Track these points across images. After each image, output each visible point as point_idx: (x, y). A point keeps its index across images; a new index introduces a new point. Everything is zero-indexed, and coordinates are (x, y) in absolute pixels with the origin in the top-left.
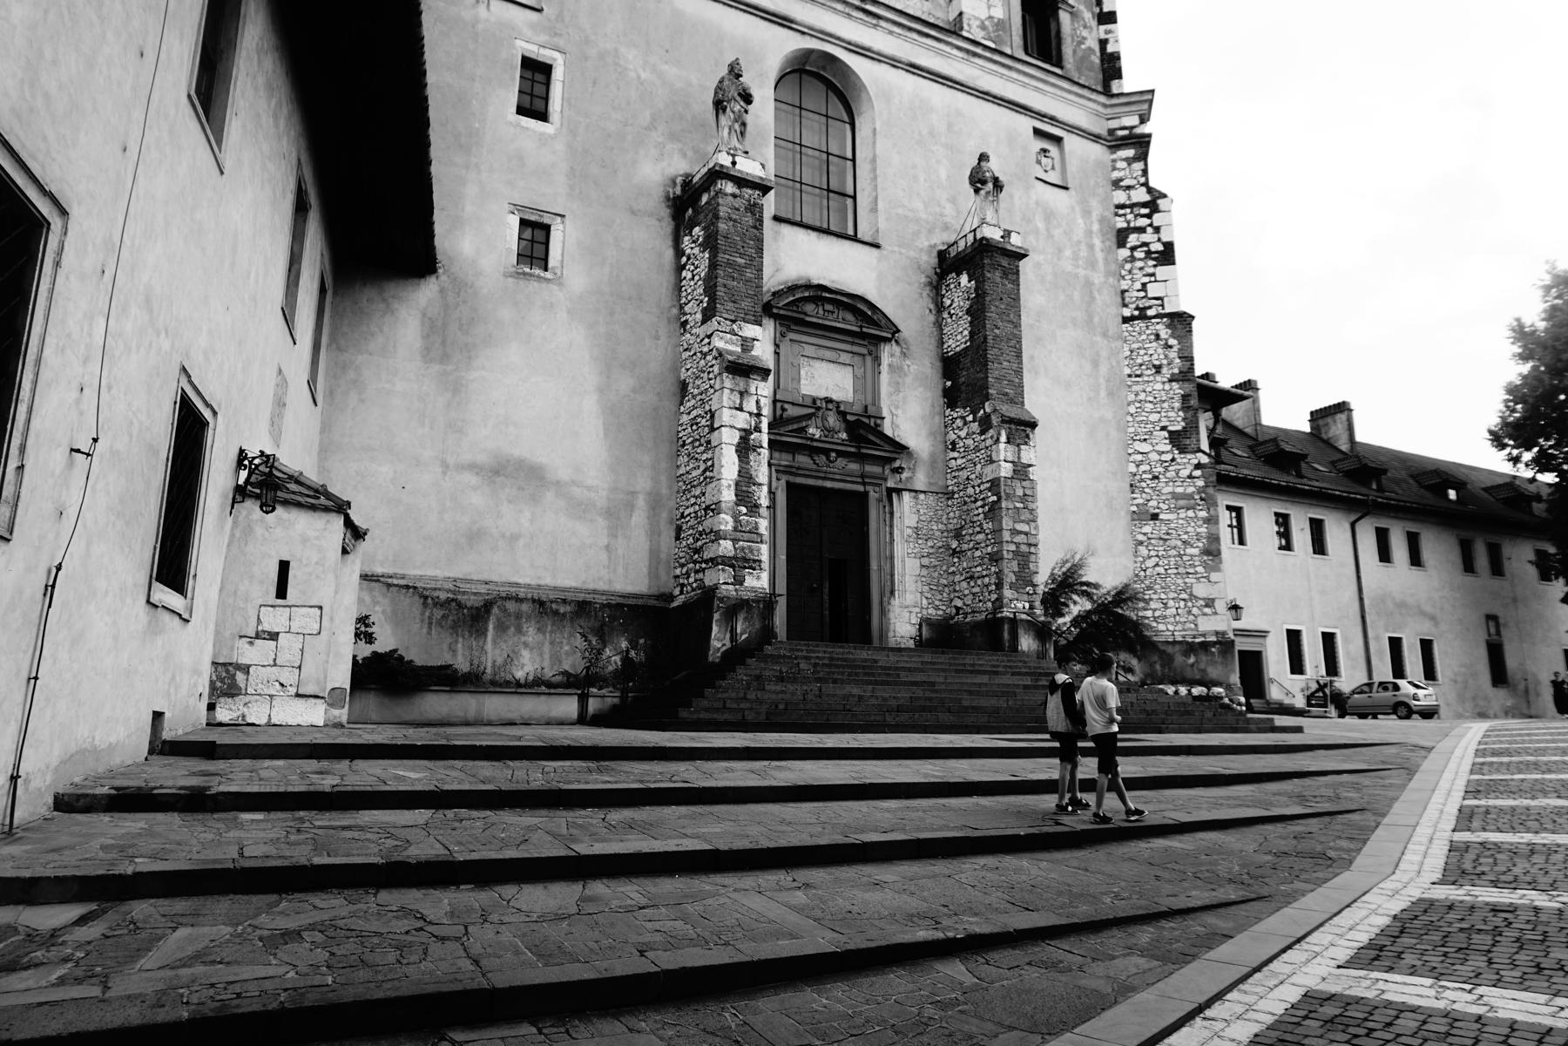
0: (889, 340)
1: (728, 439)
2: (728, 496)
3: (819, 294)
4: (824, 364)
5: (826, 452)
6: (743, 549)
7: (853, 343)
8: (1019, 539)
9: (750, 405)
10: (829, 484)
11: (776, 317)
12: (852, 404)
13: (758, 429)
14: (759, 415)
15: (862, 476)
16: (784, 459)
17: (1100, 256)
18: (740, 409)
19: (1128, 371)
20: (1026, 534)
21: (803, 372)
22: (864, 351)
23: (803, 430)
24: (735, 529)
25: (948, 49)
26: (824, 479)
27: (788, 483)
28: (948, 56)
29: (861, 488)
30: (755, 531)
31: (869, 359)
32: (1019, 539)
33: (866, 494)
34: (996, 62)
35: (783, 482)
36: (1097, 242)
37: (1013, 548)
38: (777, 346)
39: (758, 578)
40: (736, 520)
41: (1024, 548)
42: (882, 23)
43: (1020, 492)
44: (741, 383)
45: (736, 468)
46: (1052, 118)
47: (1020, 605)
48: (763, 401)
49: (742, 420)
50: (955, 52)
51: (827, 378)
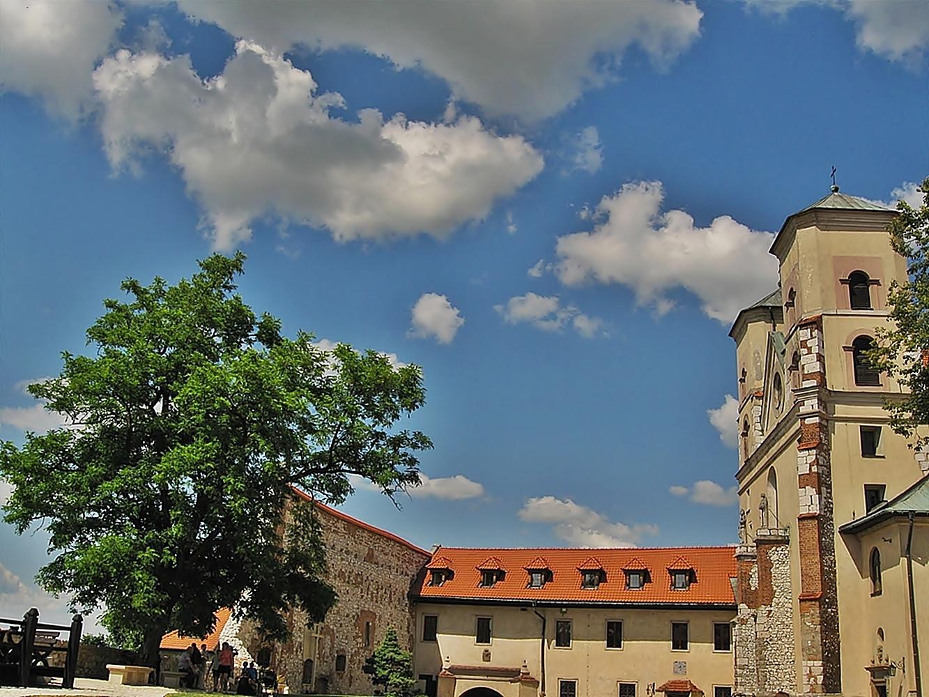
42: (776, 438)
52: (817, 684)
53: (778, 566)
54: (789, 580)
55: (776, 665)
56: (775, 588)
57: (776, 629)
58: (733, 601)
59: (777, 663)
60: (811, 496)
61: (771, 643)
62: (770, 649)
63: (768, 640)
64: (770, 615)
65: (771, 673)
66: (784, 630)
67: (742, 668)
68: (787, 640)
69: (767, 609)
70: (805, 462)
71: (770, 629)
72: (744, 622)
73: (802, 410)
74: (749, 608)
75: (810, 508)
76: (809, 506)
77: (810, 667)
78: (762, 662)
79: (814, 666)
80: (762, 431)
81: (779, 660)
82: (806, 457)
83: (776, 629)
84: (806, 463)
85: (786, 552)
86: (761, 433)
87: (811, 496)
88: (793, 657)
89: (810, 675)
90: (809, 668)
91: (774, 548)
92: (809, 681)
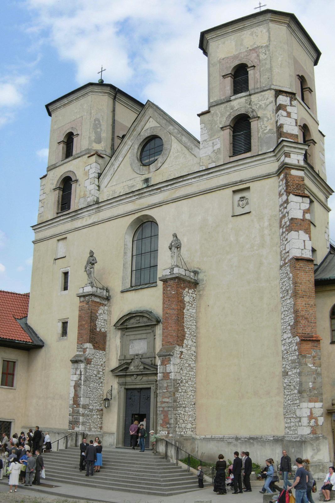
0: (155, 325)
1: (73, 384)
2: (71, 402)
3: (131, 316)
4: (137, 341)
5: (133, 375)
6: (74, 418)
7: (146, 330)
8: (163, 405)
9: (78, 372)
10: (138, 387)
11: (119, 329)
12: (146, 354)
13: (80, 379)
14: (81, 374)
15: (147, 382)
16: (122, 380)
17: (268, 239)
18: (76, 374)
19: (281, 296)
20: (167, 402)
21: (130, 347)
22: (150, 331)
23: (127, 368)
24: (73, 412)
25: (190, 181)
26: (136, 385)
27: (125, 388)
28: (191, 184)
29: (148, 386)
30: (78, 412)
31: (152, 333)
32: (163, 405)
33: (150, 388)
34: (212, 173)
35: (123, 389)
36: (266, 232)
37: (161, 409)
38: (121, 339)
39: (79, 427)
40: (73, 409)
41: (166, 409)
42: (162, 189)
43: (165, 385)
44: (76, 365)
45: (74, 393)
46: (241, 181)
47: (164, 433)
48: (82, 370)
49: (75, 378)
50: (193, 180)
51: (139, 347)
52: (317, 425)
53: (188, 308)
54: (195, 324)
55: (184, 407)
56: (186, 330)
57: (185, 372)
58: (31, 341)
59: (184, 406)
60: (304, 241)
61: (181, 385)
62: (180, 391)
63: (179, 382)
64: (182, 356)
65: (180, 415)
66: (190, 373)
67: (84, 407)
68: (191, 383)
69: (180, 350)
70: (299, 208)
71: (181, 372)
72: (88, 362)
73: (287, 160)
74: (94, 349)
75: (303, 252)
76: (302, 250)
77: (311, 409)
78: (175, 404)
79: (314, 407)
80: (99, 186)
81: (186, 403)
82: (300, 203)
83: (185, 372)
84: (300, 209)
85: (195, 296)
86: (97, 188)
87: (304, 241)
88: (194, 400)
89: (311, 417)
90: (309, 410)
91: (187, 290)
92: (309, 423)
